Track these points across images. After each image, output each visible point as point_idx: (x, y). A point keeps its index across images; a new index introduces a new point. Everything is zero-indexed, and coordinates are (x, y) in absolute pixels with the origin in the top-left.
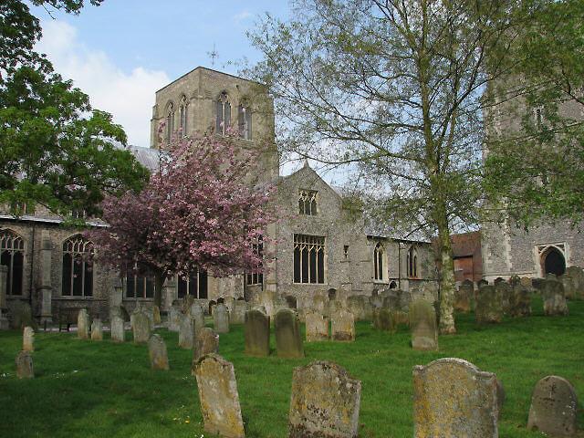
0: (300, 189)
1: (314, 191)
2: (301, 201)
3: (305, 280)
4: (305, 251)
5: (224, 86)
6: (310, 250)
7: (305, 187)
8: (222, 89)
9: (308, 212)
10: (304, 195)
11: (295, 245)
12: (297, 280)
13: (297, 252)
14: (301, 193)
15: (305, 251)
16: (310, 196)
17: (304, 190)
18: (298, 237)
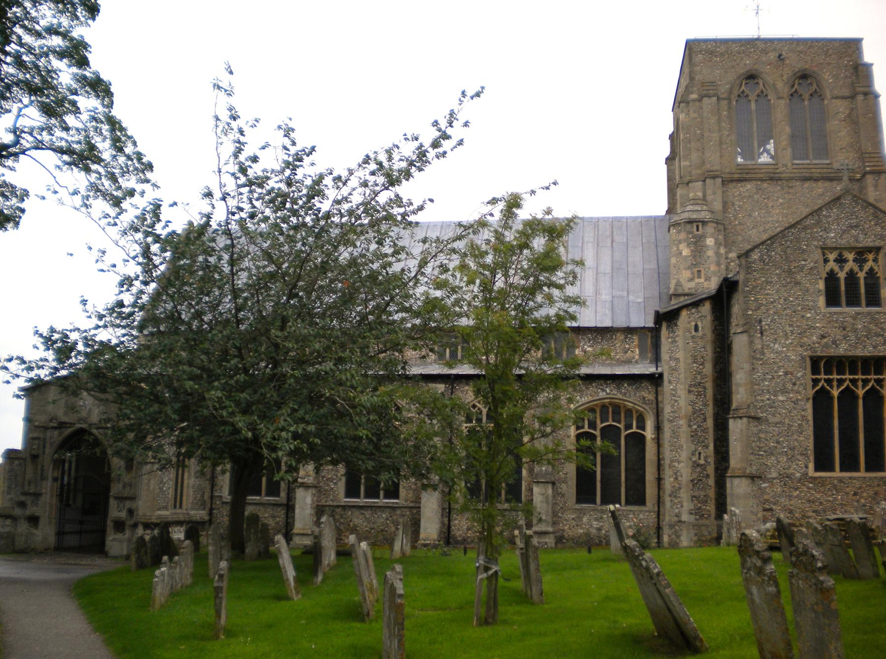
0: (824, 249)
1: (870, 250)
2: (831, 279)
3: (850, 464)
4: (848, 396)
5: (747, 63)
6: (861, 392)
7: (843, 242)
8: (742, 70)
9: (853, 301)
10: (841, 260)
11: (815, 382)
12: (823, 462)
13: (821, 399)
14: (832, 256)
15: (848, 396)
16: (860, 260)
17: (840, 249)
18: (815, 363)
